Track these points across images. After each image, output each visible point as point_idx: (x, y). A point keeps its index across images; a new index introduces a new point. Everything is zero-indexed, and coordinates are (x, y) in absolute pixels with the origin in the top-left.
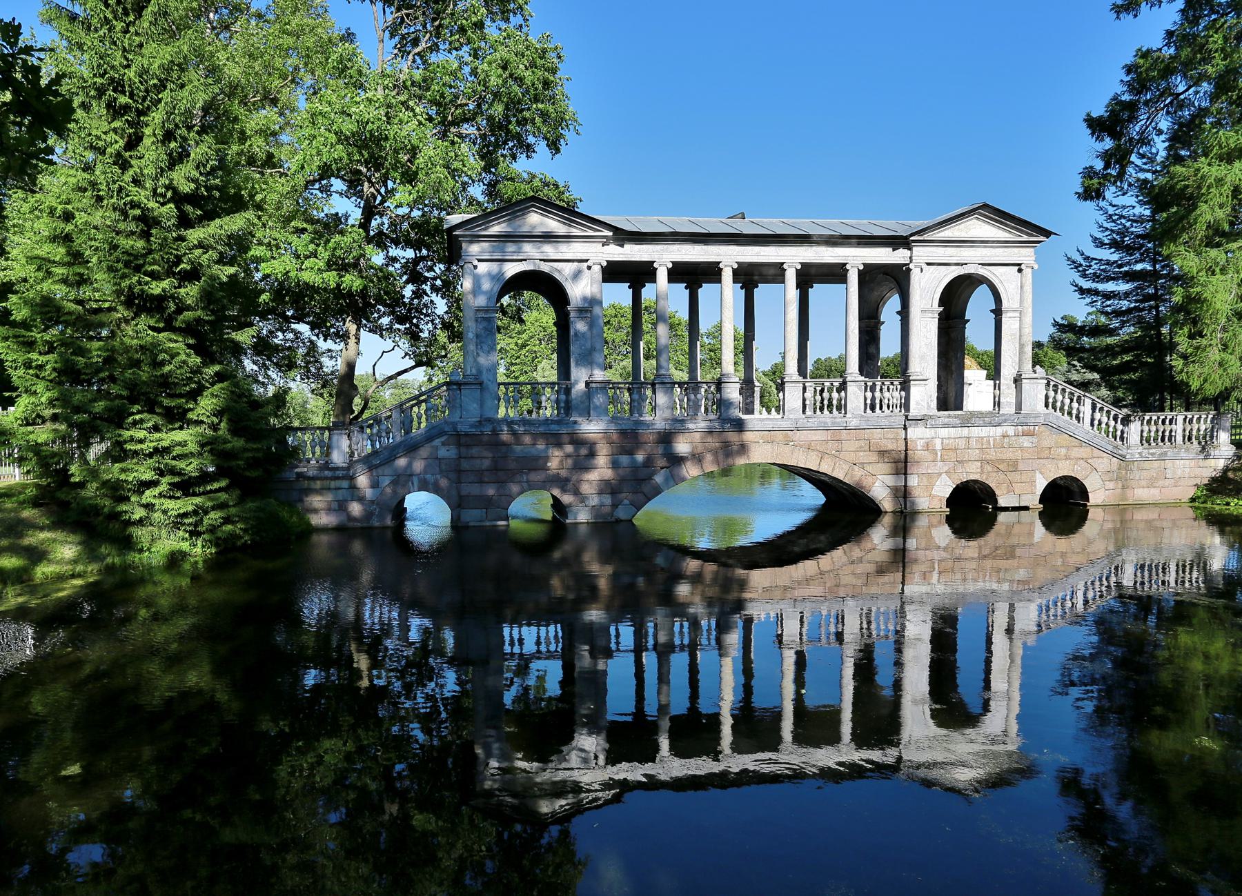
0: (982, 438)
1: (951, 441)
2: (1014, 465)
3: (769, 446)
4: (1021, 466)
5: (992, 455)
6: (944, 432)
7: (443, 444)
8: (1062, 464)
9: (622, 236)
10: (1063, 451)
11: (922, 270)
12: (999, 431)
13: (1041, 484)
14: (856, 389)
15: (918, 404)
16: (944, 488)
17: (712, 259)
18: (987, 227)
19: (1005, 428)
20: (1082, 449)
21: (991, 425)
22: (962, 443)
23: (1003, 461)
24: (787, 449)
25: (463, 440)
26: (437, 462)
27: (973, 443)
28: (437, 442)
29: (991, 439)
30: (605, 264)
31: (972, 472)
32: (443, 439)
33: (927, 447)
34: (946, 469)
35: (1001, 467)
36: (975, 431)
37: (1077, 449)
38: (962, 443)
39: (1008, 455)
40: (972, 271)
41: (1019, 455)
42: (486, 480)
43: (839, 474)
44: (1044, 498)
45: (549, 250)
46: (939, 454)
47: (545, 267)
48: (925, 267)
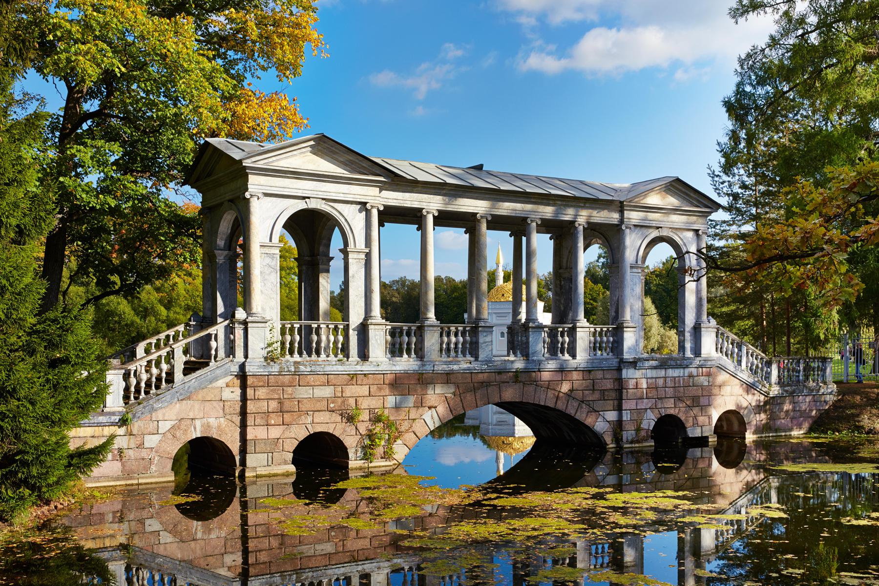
0: (675, 378)
1: (654, 380)
7: (227, 386)
9: (396, 181)
16: (649, 421)
22: (661, 382)
25: (250, 381)
26: (221, 404)
27: (670, 383)
28: (221, 383)
29: (681, 379)
30: (382, 208)
34: (649, 405)
36: (672, 373)
38: (661, 382)
42: (273, 422)
44: (718, 429)
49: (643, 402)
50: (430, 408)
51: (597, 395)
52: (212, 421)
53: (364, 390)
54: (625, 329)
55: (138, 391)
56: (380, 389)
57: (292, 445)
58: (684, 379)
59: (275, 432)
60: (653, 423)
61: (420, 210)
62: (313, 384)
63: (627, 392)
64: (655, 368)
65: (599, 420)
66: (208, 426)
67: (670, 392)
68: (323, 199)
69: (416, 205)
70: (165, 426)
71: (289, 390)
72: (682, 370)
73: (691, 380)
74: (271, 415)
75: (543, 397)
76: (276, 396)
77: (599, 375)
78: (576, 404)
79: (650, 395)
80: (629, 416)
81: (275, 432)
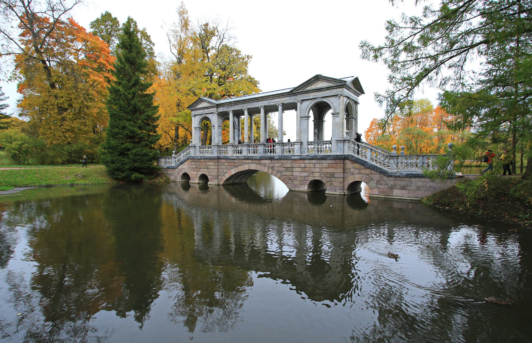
2: (332, 175)
3: (254, 165)
4: (336, 175)
8: (357, 176)
11: (301, 103)
14: (279, 146)
15: (297, 151)
17: (241, 108)
18: (324, 82)
23: (327, 173)
24: (259, 165)
35: (328, 175)
37: (363, 170)
45: (206, 111)
47: (207, 116)
48: (301, 101)
53: (212, 164)
59: (195, 173)
69: (226, 110)
75: (263, 169)
77: (285, 161)
78: (276, 172)
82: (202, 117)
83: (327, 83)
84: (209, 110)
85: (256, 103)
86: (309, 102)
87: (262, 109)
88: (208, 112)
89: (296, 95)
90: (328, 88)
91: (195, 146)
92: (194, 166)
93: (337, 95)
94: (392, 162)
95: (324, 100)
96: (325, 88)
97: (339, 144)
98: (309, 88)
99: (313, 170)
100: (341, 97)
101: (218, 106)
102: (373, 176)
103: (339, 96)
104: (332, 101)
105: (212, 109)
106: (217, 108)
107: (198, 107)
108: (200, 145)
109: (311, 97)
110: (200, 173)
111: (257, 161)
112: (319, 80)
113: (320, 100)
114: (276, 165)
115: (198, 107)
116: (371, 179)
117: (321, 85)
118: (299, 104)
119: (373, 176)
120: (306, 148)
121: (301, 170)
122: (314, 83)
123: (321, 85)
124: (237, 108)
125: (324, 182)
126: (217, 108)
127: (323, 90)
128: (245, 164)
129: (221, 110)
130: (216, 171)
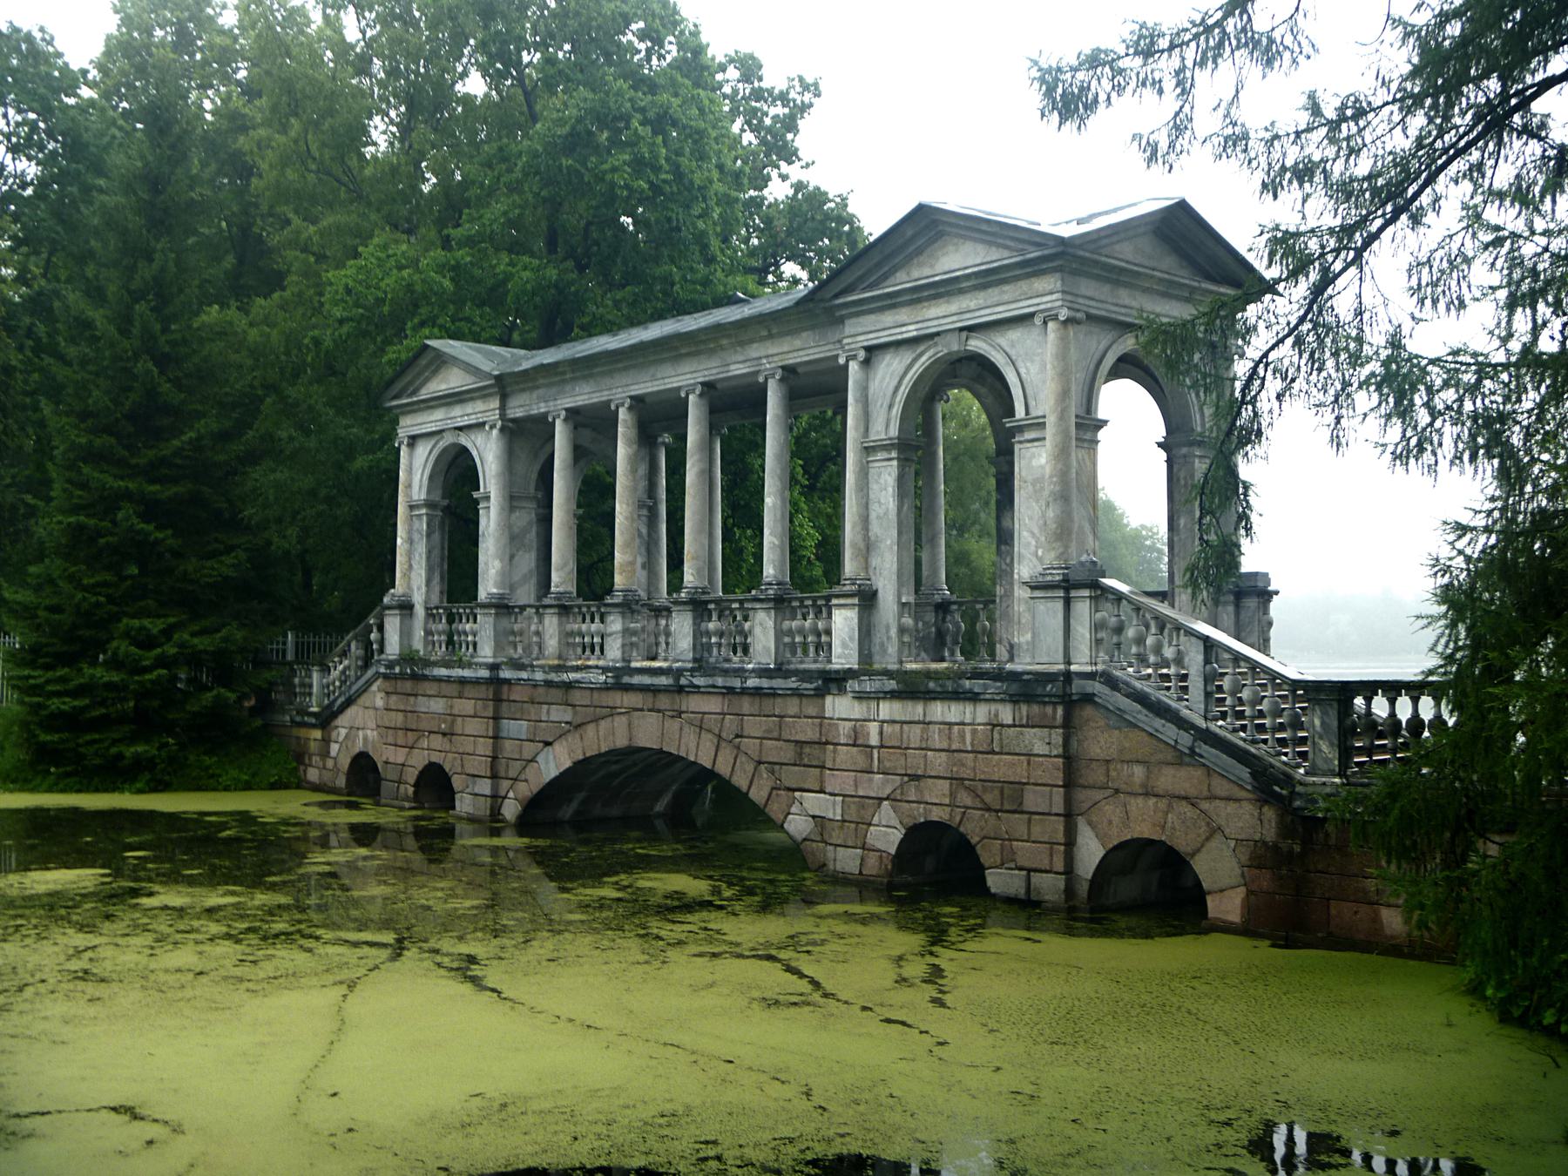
0: (950, 724)
1: (897, 727)
2: (1011, 797)
4: (1033, 800)
5: (970, 766)
6: (886, 709)
8: (1136, 804)
10: (1139, 771)
12: (982, 712)
13: (1091, 852)
15: (844, 645)
16: (887, 834)
17: (601, 397)
18: (968, 247)
19: (994, 707)
20: (1183, 772)
21: (958, 696)
24: (673, 725)
27: (937, 740)
28: (374, 688)
31: (935, 804)
32: (379, 682)
33: (857, 741)
34: (888, 791)
35: (988, 798)
36: (941, 711)
39: (1001, 768)
40: (955, 348)
41: (1019, 772)
42: (399, 743)
43: (740, 781)
46: (875, 752)
48: (862, 355)
49: (871, 780)
50: (548, 744)
51: (788, 754)
52: (369, 732)
53: (466, 706)
54: (835, 601)
55: (334, 692)
56: (485, 707)
57: (411, 776)
58: (974, 732)
60: (897, 836)
61: (545, 415)
62: (429, 692)
63: (835, 751)
64: (893, 695)
65: (793, 810)
66: (365, 739)
67: (939, 762)
68: (456, 428)
70: (343, 732)
71: (412, 699)
72: (969, 708)
73: (996, 736)
74: (400, 732)
76: (402, 708)
78: (750, 768)
79: (887, 764)
80: (839, 811)
81: (399, 756)
82: (442, 445)
83: (980, 248)
84: (469, 408)
85: (667, 370)
86: (906, 356)
87: (691, 397)
88: (465, 421)
89: (841, 321)
90: (987, 279)
91: (406, 607)
92: (399, 719)
93: (1031, 315)
94: (1317, 722)
95: (977, 344)
96: (968, 277)
97: (1041, 607)
98: (901, 281)
99: (915, 762)
100: (1051, 325)
101: (503, 386)
102: (1224, 813)
103: (1038, 321)
104: (1012, 353)
105: (479, 406)
106: (504, 398)
107: (424, 393)
108: (435, 600)
109: (911, 331)
110: (419, 760)
111: (664, 701)
112: (949, 234)
113: (953, 345)
114: (754, 726)
115: (424, 393)
116: (1215, 831)
117: (957, 259)
118: (854, 367)
119: (1224, 813)
120: (893, 632)
121: (861, 762)
122: (919, 252)
123: (957, 259)
124: (583, 395)
125: (974, 840)
126: (504, 398)
127: (962, 292)
128: (612, 712)
129: (521, 407)
130: (484, 747)
